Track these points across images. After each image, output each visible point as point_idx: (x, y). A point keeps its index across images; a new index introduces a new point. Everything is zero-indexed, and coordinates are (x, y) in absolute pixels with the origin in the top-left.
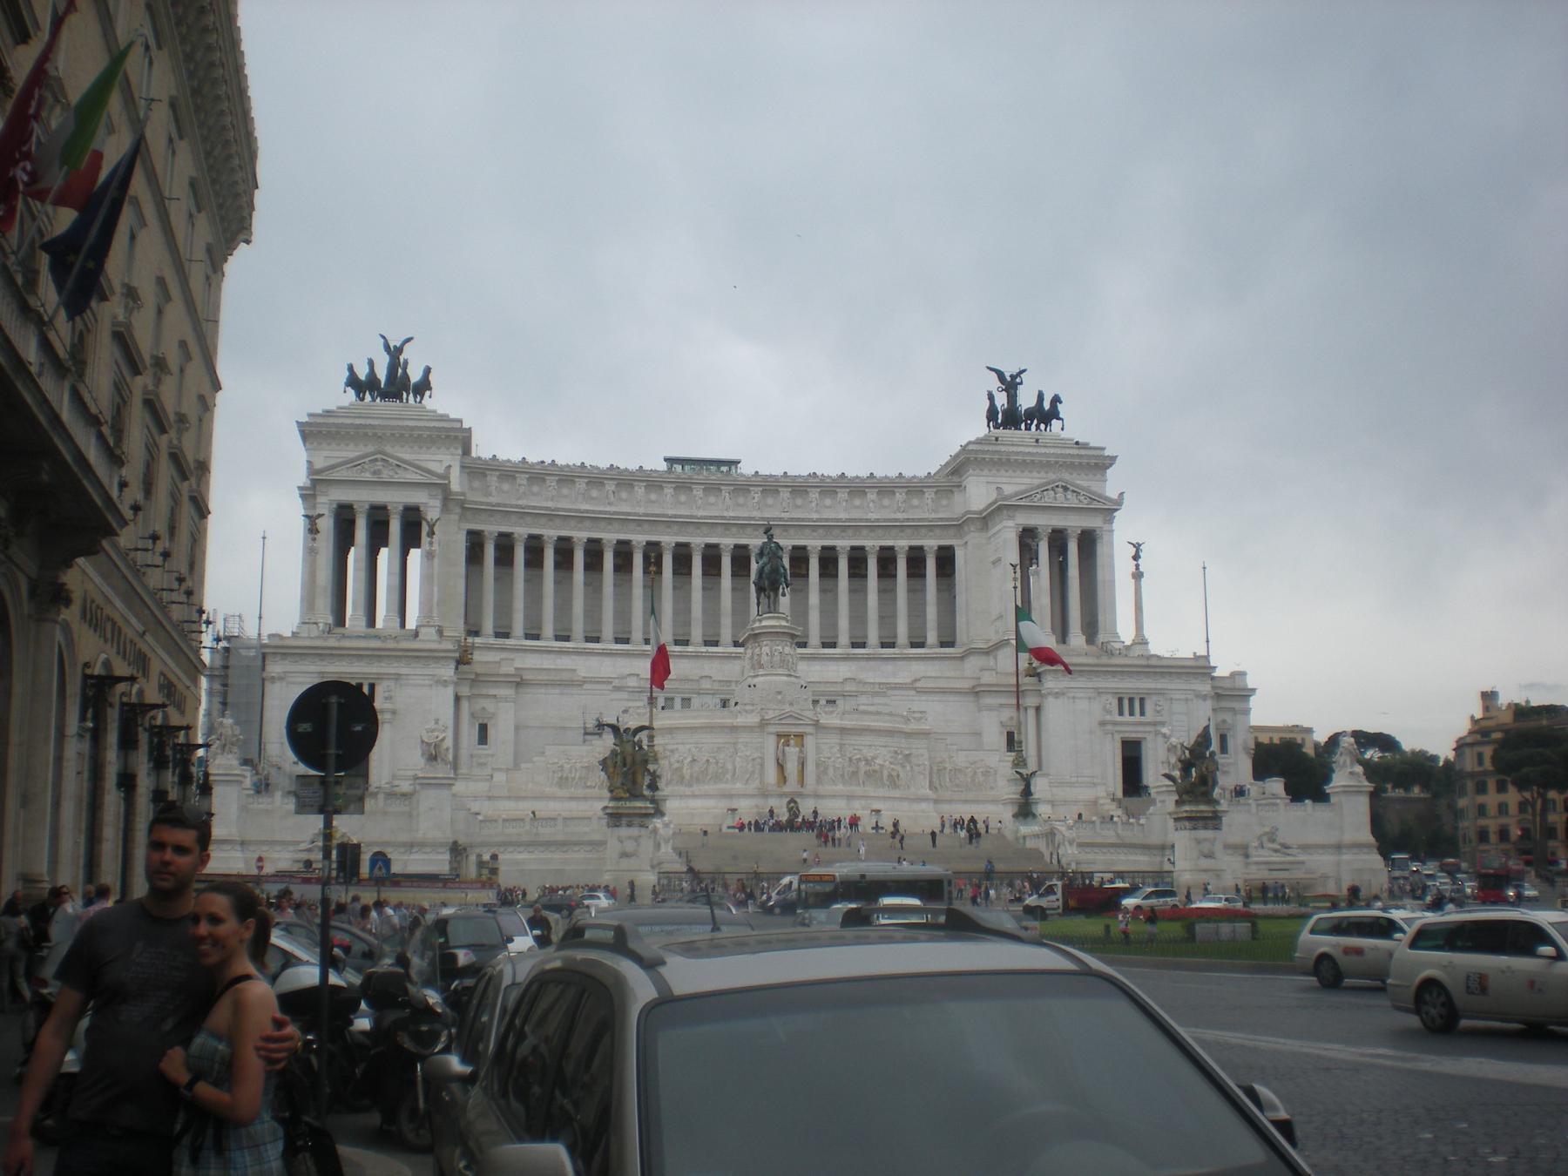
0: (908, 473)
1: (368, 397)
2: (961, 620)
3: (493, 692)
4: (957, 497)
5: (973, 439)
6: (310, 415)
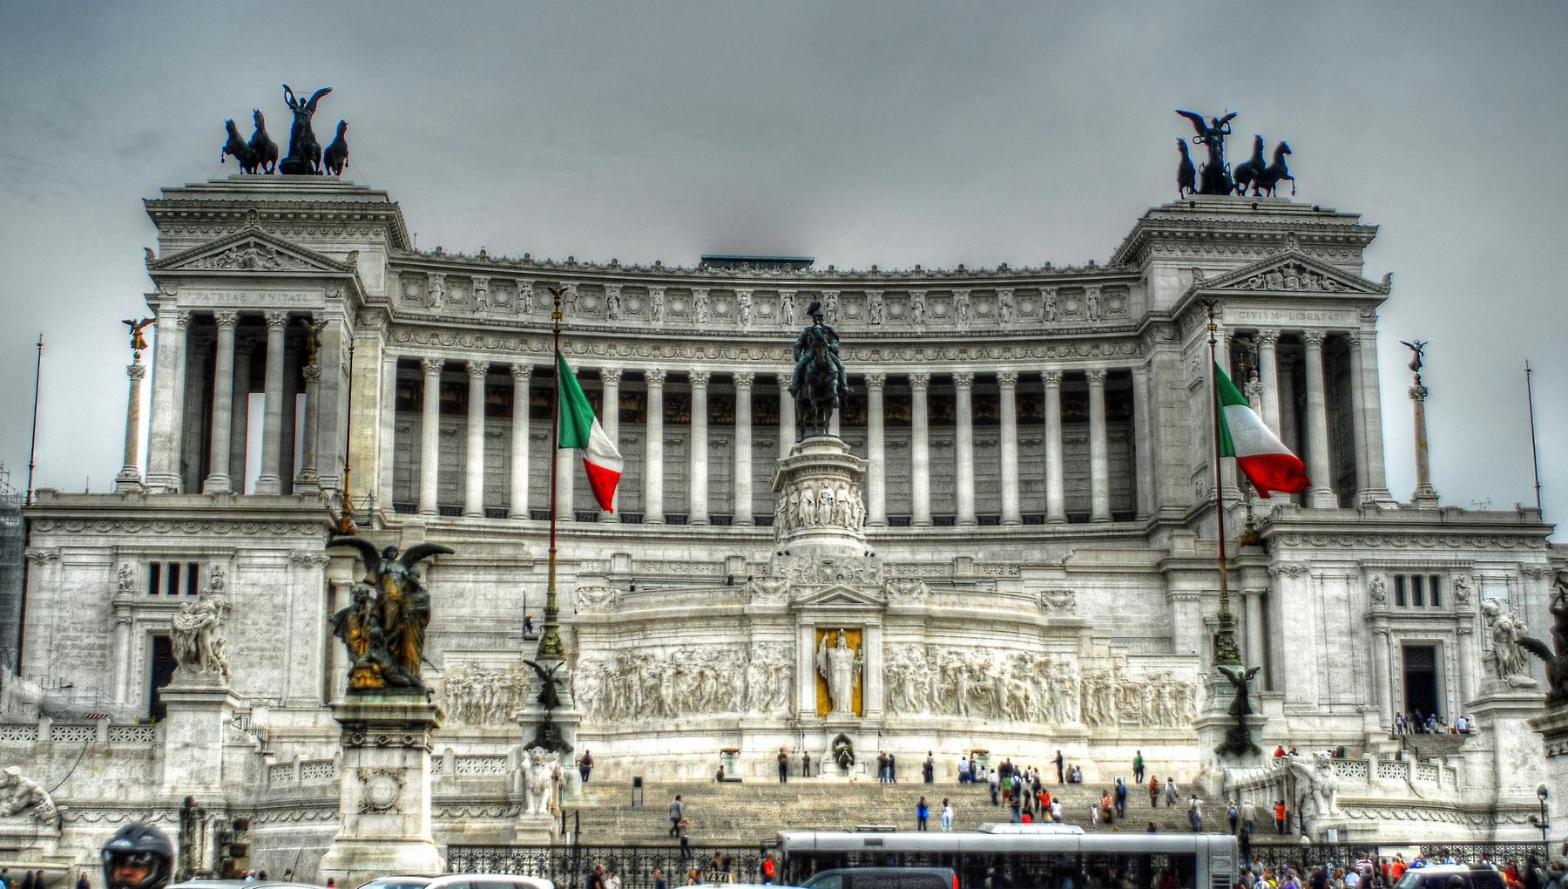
1: (260, 169)
2: (1144, 480)
4: (1136, 297)
5: (1158, 205)
6: (165, 191)
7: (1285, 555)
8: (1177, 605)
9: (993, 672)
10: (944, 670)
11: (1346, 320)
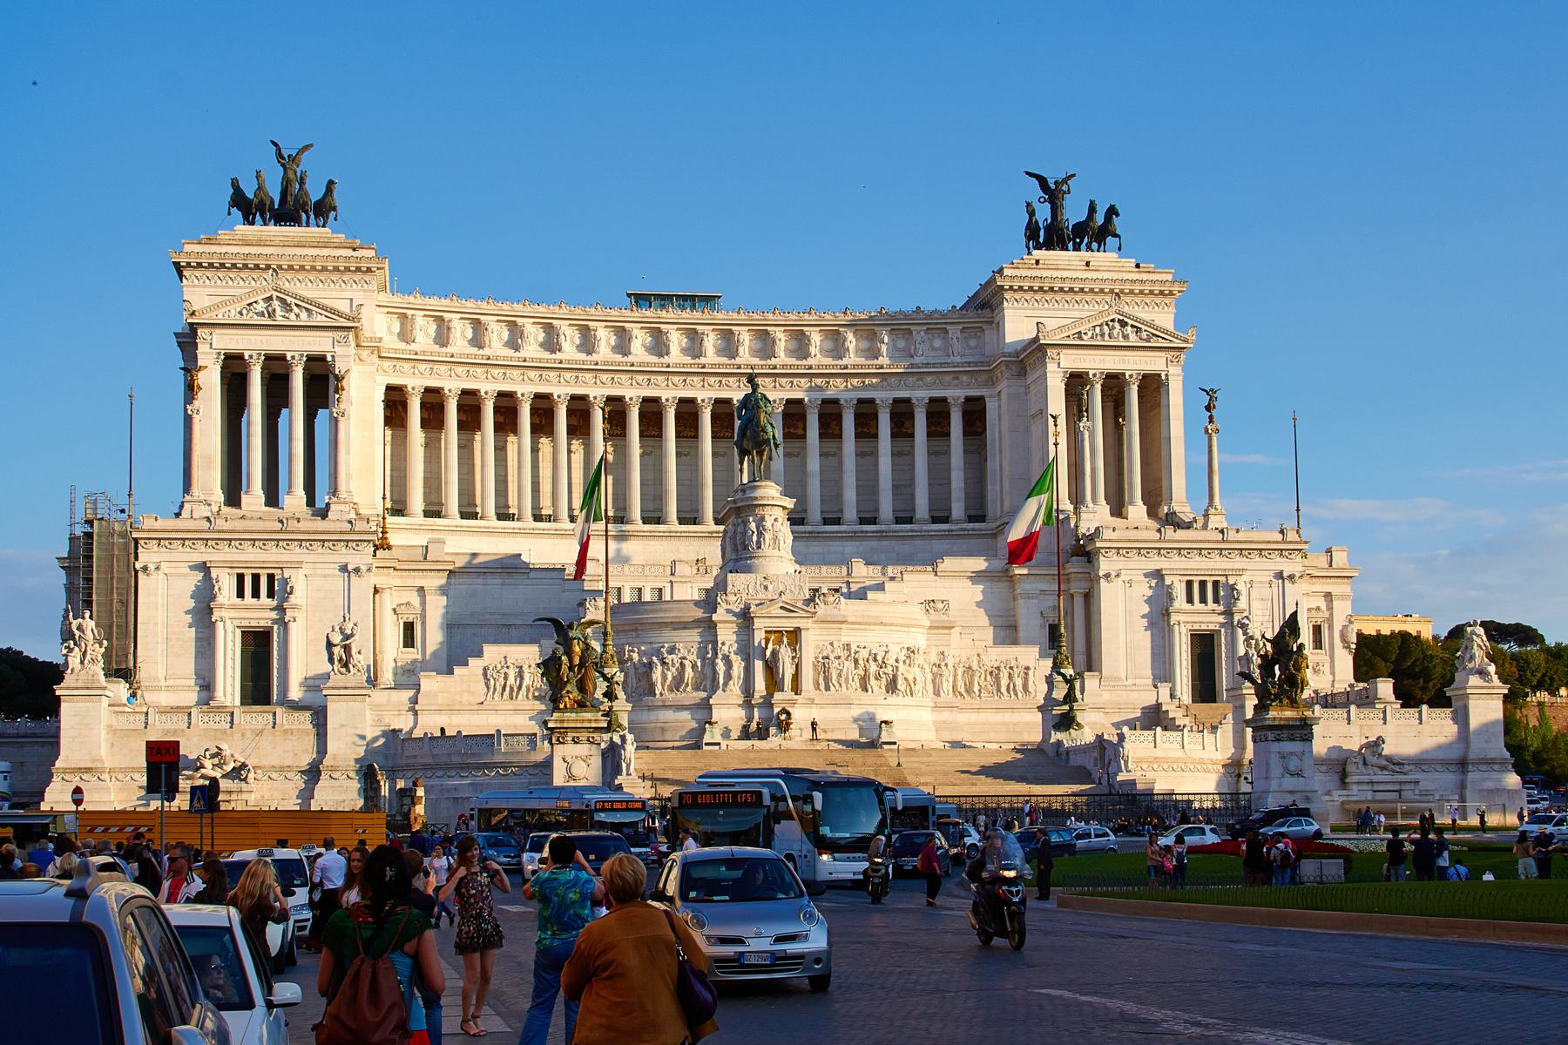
0: (928, 307)
3: (419, 583)
4: (989, 335)
7: (1105, 565)
8: (1021, 602)
9: (891, 661)
10: (856, 661)
11: (1153, 363)
